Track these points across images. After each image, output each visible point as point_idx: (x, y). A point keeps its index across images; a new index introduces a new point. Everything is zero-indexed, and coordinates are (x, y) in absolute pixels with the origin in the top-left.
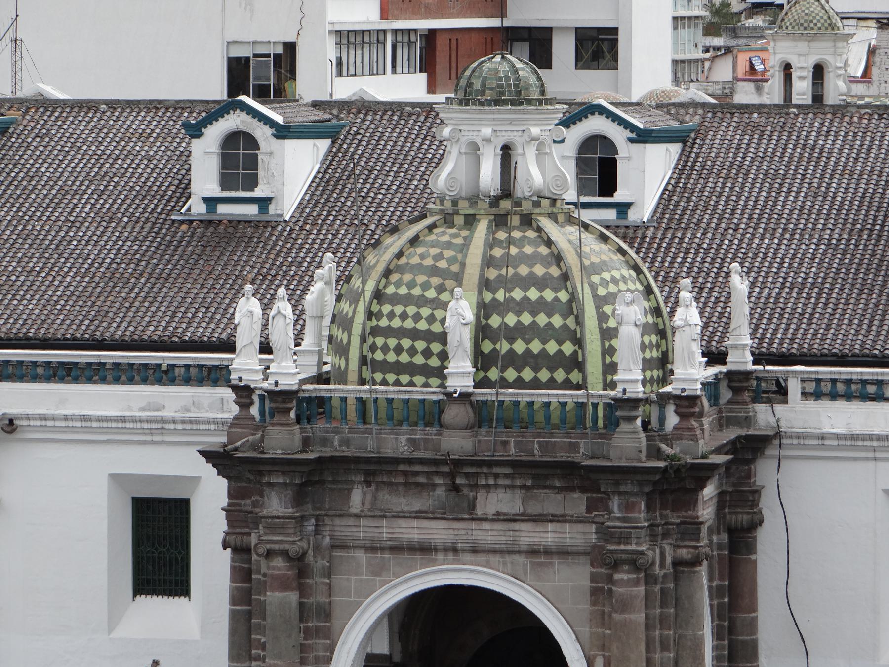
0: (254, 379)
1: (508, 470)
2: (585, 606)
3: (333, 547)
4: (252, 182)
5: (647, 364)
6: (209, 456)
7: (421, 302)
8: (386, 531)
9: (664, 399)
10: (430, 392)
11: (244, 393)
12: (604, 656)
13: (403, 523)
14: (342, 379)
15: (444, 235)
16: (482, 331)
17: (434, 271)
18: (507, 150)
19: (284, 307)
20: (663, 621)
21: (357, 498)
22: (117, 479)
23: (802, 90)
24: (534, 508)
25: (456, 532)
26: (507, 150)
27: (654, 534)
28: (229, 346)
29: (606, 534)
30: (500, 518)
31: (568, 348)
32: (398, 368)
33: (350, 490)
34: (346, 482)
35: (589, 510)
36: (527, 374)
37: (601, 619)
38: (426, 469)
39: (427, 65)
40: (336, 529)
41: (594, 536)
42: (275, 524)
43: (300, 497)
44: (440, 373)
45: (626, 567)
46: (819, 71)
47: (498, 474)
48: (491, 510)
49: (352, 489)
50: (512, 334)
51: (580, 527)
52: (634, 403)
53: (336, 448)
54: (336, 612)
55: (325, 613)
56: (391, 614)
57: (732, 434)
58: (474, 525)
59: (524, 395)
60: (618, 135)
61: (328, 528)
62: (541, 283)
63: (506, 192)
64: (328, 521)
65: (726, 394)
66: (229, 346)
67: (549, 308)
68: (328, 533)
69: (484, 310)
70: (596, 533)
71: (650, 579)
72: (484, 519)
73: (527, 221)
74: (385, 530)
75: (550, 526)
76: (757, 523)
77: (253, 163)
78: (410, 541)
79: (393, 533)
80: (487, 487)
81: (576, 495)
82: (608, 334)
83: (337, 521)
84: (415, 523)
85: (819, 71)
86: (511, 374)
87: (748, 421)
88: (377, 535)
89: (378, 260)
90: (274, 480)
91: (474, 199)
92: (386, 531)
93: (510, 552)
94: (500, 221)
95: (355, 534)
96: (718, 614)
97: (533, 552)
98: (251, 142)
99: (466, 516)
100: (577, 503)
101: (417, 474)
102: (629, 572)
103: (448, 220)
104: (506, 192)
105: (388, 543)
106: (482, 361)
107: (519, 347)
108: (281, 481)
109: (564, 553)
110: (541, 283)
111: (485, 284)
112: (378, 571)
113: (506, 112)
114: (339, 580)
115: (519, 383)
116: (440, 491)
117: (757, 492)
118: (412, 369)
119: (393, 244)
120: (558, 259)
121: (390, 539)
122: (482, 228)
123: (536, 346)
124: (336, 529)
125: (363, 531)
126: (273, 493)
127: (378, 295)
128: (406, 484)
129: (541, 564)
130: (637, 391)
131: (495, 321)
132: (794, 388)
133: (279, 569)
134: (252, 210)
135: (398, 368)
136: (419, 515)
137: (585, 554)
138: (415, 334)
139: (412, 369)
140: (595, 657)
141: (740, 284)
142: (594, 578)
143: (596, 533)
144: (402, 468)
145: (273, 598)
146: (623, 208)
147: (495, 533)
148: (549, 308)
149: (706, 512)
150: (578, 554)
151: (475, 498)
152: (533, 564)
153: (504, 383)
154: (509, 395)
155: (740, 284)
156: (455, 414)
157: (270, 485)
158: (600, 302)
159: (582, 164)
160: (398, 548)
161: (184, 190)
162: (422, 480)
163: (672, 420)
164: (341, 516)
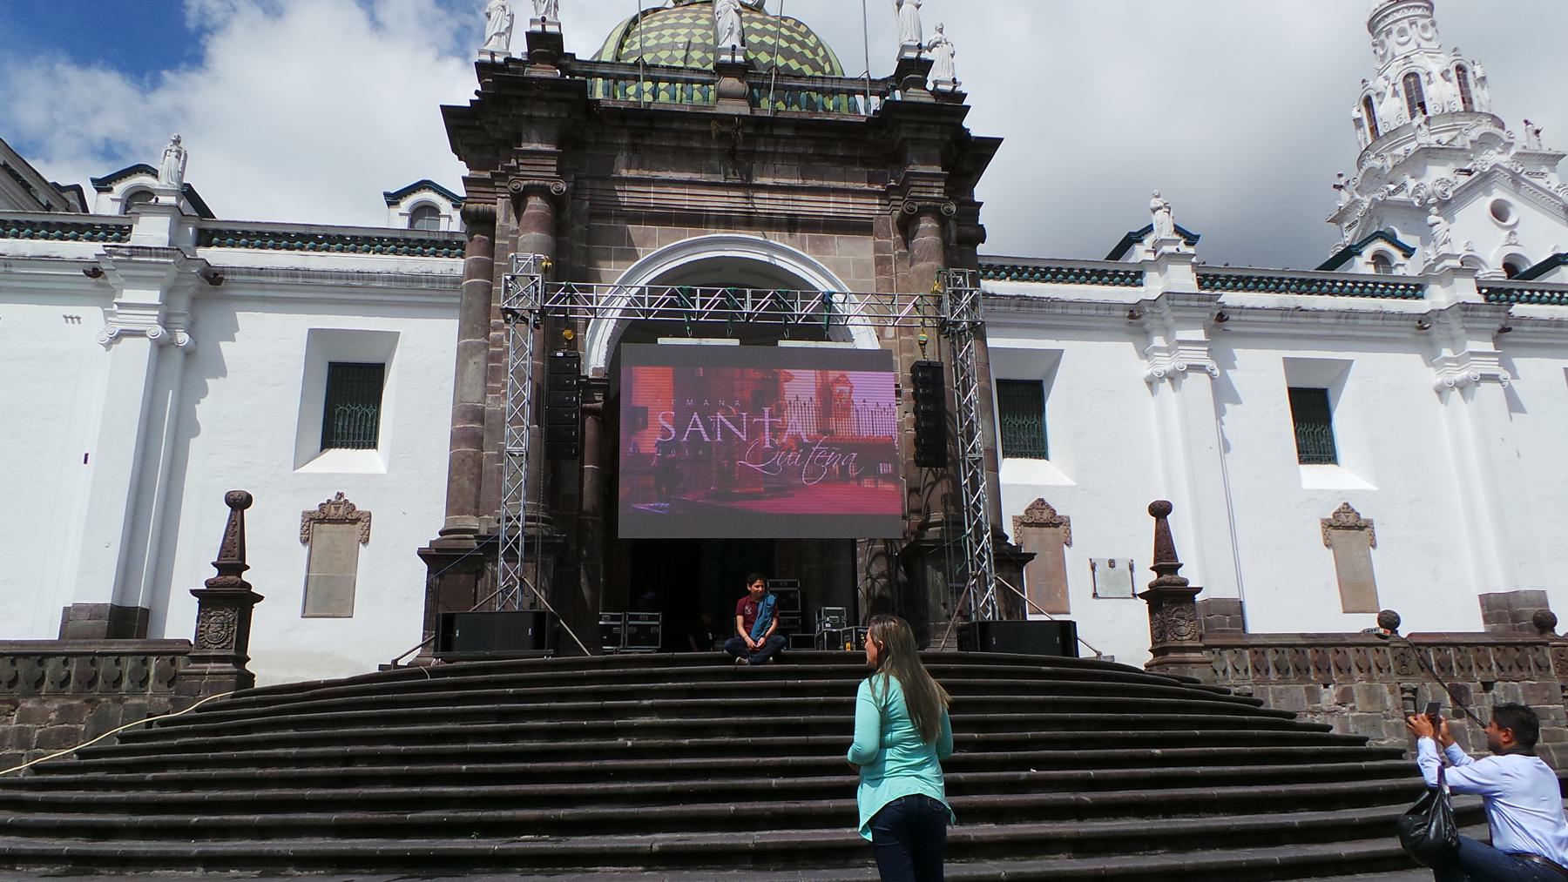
1: (789, 133)
2: (872, 279)
3: (593, 216)
40: (597, 193)
47: (779, 137)
49: (615, 156)
64: (588, 183)
80: (764, 156)
83: (598, 185)
101: (691, 135)
102: (929, 222)
124: (597, 193)
126: (533, 131)
129: (821, 239)
133: (537, 208)
144: (676, 125)
157: (531, 119)
162: (696, 144)
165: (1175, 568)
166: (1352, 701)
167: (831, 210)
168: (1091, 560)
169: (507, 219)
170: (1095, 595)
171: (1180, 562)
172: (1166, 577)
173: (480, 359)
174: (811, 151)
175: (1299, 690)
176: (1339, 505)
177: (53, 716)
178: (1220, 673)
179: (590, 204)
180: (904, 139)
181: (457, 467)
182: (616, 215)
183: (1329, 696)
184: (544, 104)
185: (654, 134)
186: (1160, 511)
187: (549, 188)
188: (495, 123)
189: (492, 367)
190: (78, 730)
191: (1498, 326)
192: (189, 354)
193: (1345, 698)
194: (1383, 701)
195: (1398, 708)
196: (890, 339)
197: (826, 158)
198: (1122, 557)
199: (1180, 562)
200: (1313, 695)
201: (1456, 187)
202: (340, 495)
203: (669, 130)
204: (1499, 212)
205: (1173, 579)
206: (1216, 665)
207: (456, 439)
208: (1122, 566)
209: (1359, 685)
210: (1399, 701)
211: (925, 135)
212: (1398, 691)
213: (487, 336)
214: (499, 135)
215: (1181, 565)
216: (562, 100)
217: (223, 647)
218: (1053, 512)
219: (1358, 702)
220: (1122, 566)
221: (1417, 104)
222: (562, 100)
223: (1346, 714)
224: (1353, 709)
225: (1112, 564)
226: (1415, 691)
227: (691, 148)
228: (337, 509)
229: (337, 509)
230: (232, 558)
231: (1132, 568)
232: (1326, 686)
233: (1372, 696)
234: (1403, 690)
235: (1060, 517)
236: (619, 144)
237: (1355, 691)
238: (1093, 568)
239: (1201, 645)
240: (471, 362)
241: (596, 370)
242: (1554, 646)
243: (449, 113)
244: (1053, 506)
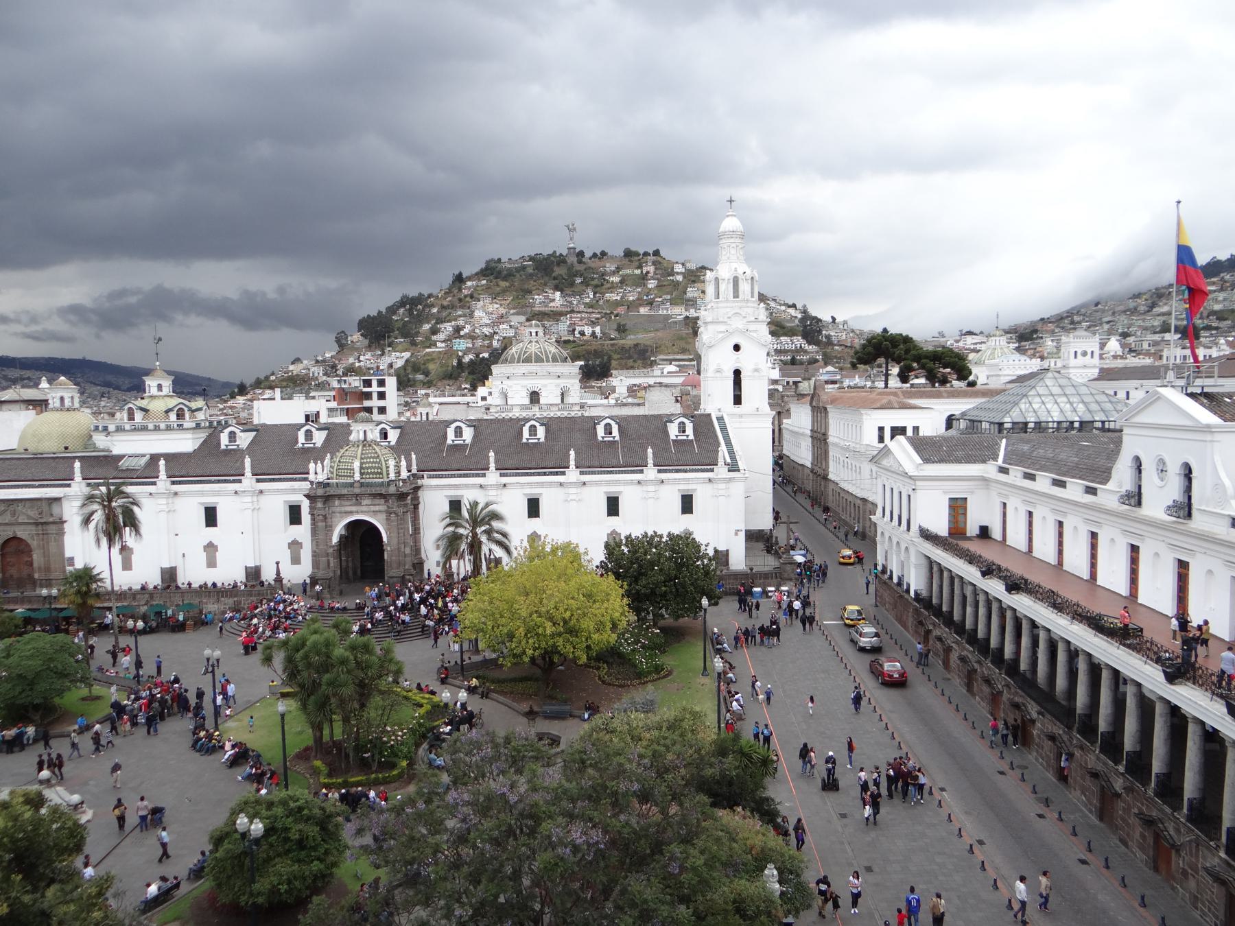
0: (313, 480)
4: (311, 440)
5: (396, 473)
6: (305, 496)
7: (349, 462)
8: (343, 509)
9: (399, 480)
10: (352, 481)
11: (312, 483)
14: (332, 478)
15: (353, 449)
16: (361, 468)
17: (351, 456)
18: (365, 431)
19: (319, 464)
20: (401, 524)
21: (337, 502)
22: (285, 501)
23: (424, 418)
24: (374, 503)
26: (365, 431)
27: (399, 507)
28: (308, 473)
29: (388, 507)
30: (366, 505)
31: (379, 470)
32: (344, 476)
36: (371, 476)
37: (389, 524)
39: (347, 415)
42: (319, 510)
43: (324, 504)
44: (353, 477)
46: (427, 414)
50: (368, 468)
52: (393, 481)
53: (332, 493)
55: (331, 526)
56: (345, 526)
57: (413, 486)
59: (370, 480)
60: (387, 427)
62: (373, 458)
63: (365, 440)
65: (412, 478)
66: (308, 473)
67: (375, 463)
69: (362, 464)
71: (397, 515)
73: (370, 445)
76: (419, 504)
77: (311, 436)
82: (387, 467)
85: (427, 414)
86: (368, 476)
87: (417, 483)
89: (339, 455)
91: (359, 441)
92: (343, 509)
94: (364, 446)
96: (412, 522)
98: (311, 431)
100: (382, 501)
103: (353, 446)
104: (365, 440)
106: (362, 474)
107: (369, 471)
109: (380, 511)
110: (373, 458)
111: (362, 458)
112: (342, 517)
113: (364, 424)
114: (334, 519)
115: (370, 478)
117: (419, 497)
118: (347, 476)
119: (342, 451)
120: (376, 453)
122: (361, 447)
123: (373, 470)
125: (338, 509)
127: (339, 462)
130: (394, 478)
131: (364, 466)
132: (425, 476)
134: (312, 445)
135: (344, 476)
138: (347, 469)
139: (347, 476)
141: (414, 456)
145: (320, 524)
146: (389, 442)
148: (375, 463)
149: (409, 502)
153: (366, 478)
154: (367, 480)
155: (414, 456)
156: (356, 485)
158: (385, 461)
159: (381, 434)
160: (346, 512)
161: (297, 442)
163: (401, 484)
181: (313, 562)
192: (259, 508)
207: (313, 556)
230: (278, 573)
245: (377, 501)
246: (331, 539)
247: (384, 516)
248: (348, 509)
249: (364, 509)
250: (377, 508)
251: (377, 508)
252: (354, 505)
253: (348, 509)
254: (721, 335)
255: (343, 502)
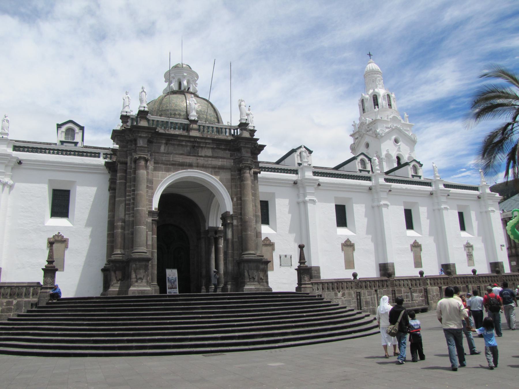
8: (171, 158)
12: (236, 197)
13: (177, 156)
21: (163, 149)
24: (216, 155)
25: (193, 160)
30: (206, 157)
33: (160, 146)
34: (159, 143)
35: (231, 156)
38: (187, 139)
40: (156, 157)
41: (233, 163)
43: (150, 142)
45: (247, 168)
47: (207, 143)
48: (203, 155)
51: (229, 161)
54: (154, 183)
58: (198, 158)
61: (154, 156)
64: (154, 154)
68: (153, 158)
70: (233, 162)
72: (201, 156)
74: (171, 158)
75: (220, 160)
78: (179, 161)
79: (174, 159)
80: (202, 147)
81: (227, 152)
83: (157, 154)
84: (181, 156)
88: (169, 159)
90: (142, 135)
92: (171, 158)
93: (208, 167)
95: (162, 159)
97: (214, 167)
99: (196, 155)
100: (227, 154)
101: (183, 141)
105: (172, 162)
108: (145, 136)
116: (188, 148)
121: (172, 161)
126: (141, 140)
128: (178, 145)
129: (217, 172)
136: (182, 154)
137: (230, 169)
140: (234, 197)
142: (232, 175)
143: (233, 162)
144: (179, 138)
147: (204, 161)
150: (226, 169)
151: (198, 151)
152: (214, 171)
157: (141, 137)
162: (184, 143)
164: (158, 153)
165: (304, 263)
166: (345, 296)
167: (220, 164)
168: (280, 255)
169: (131, 163)
170: (281, 265)
171: (306, 261)
172: (302, 265)
173: (123, 204)
174: (215, 147)
175: (332, 293)
176: (346, 239)
177: (5, 304)
178: (314, 290)
179: (154, 160)
180: (241, 146)
182: (161, 163)
183: (340, 294)
184: (145, 133)
185: (172, 140)
186: (301, 247)
187: (145, 157)
188: (129, 135)
189: (128, 207)
190: (11, 308)
191: (388, 190)
193: (343, 295)
194: (352, 295)
195: (355, 297)
196: (235, 201)
197: (219, 149)
198: (288, 253)
199: (306, 261)
200: (336, 295)
201: (385, 132)
202: (59, 233)
203: (177, 139)
204: (396, 141)
205: (304, 265)
206: (314, 288)
208: (288, 257)
209: (346, 291)
210: (356, 295)
211: (247, 146)
212: (356, 293)
213: (125, 197)
214: (129, 139)
215: (306, 262)
216: (150, 132)
217: (51, 285)
218: (270, 241)
219: (346, 296)
220: (288, 257)
221: (376, 103)
222: (150, 132)
223: (343, 299)
224: (345, 298)
225: (286, 256)
226: (359, 293)
227: (182, 145)
228: (58, 237)
229: (58, 237)
231: (291, 257)
232: (339, 292)
233: (350, 294)
234: (357, 293)
235: (272, 242)
236: (162, 143)
237: (346, 293)
238: (280, 257)
239: (310, 283)
240: (121, 205)
241: (155, 209)
242: (391, 280)
243: (115, 132)
244: (271, 239)
245: (221, 153)
246: (151, 201)
247: (227, 175)
248: (180, 159)
249: (201, 161)
250: (219, 162)
251: (219, 162)
252: (189, 154)
253: (180, 159)
254: (387, 130)
255: (171, 148)
